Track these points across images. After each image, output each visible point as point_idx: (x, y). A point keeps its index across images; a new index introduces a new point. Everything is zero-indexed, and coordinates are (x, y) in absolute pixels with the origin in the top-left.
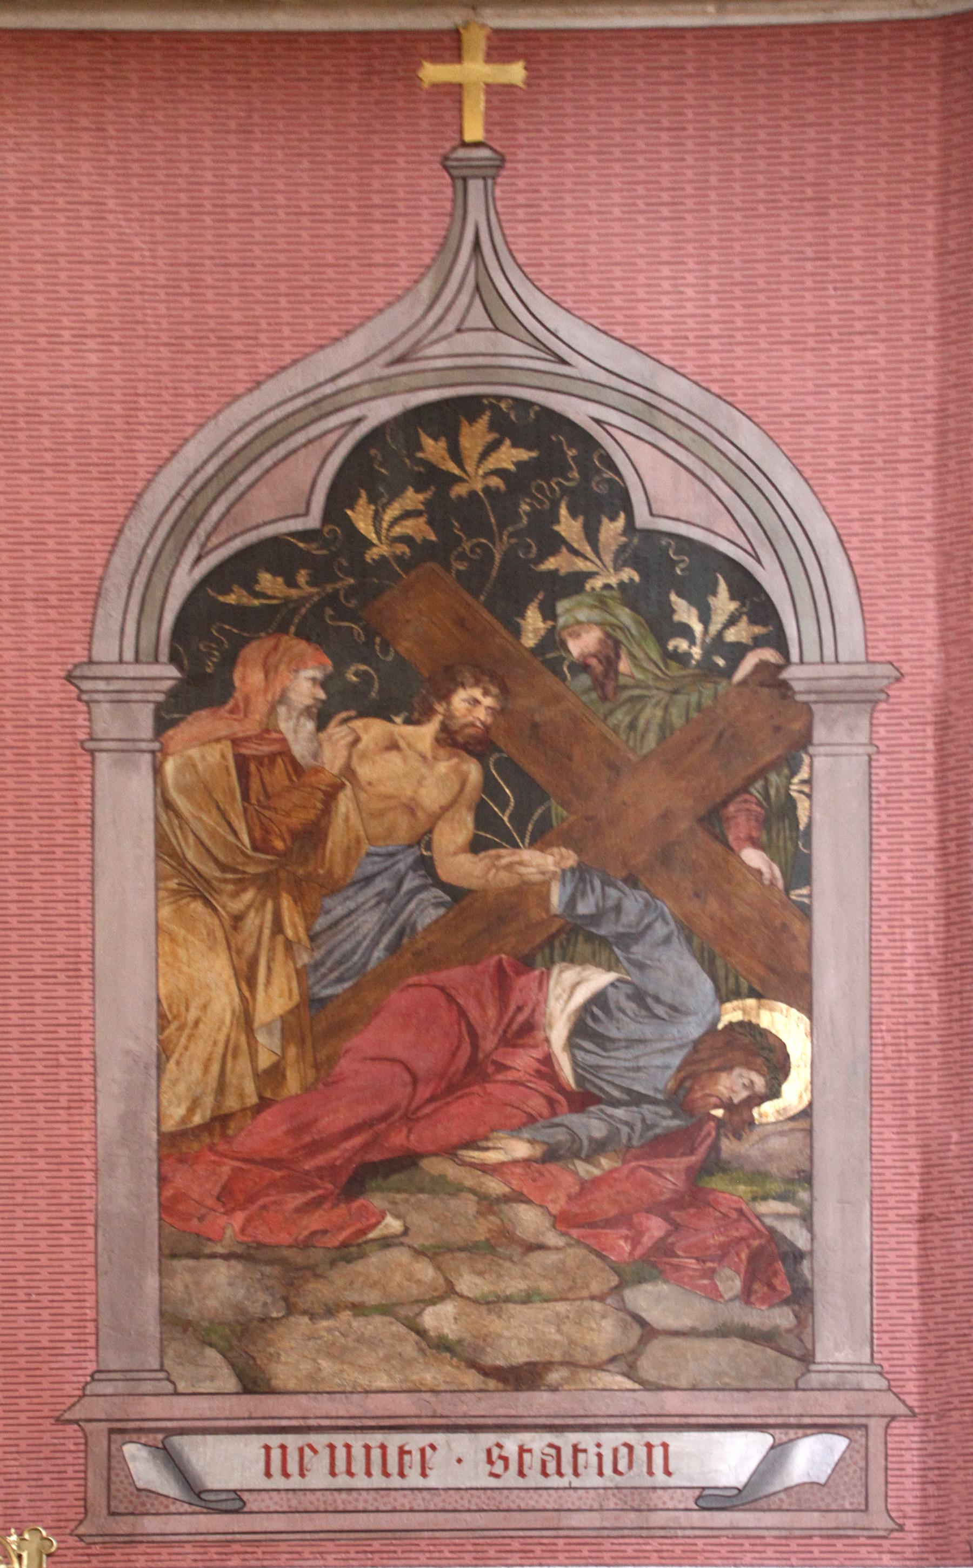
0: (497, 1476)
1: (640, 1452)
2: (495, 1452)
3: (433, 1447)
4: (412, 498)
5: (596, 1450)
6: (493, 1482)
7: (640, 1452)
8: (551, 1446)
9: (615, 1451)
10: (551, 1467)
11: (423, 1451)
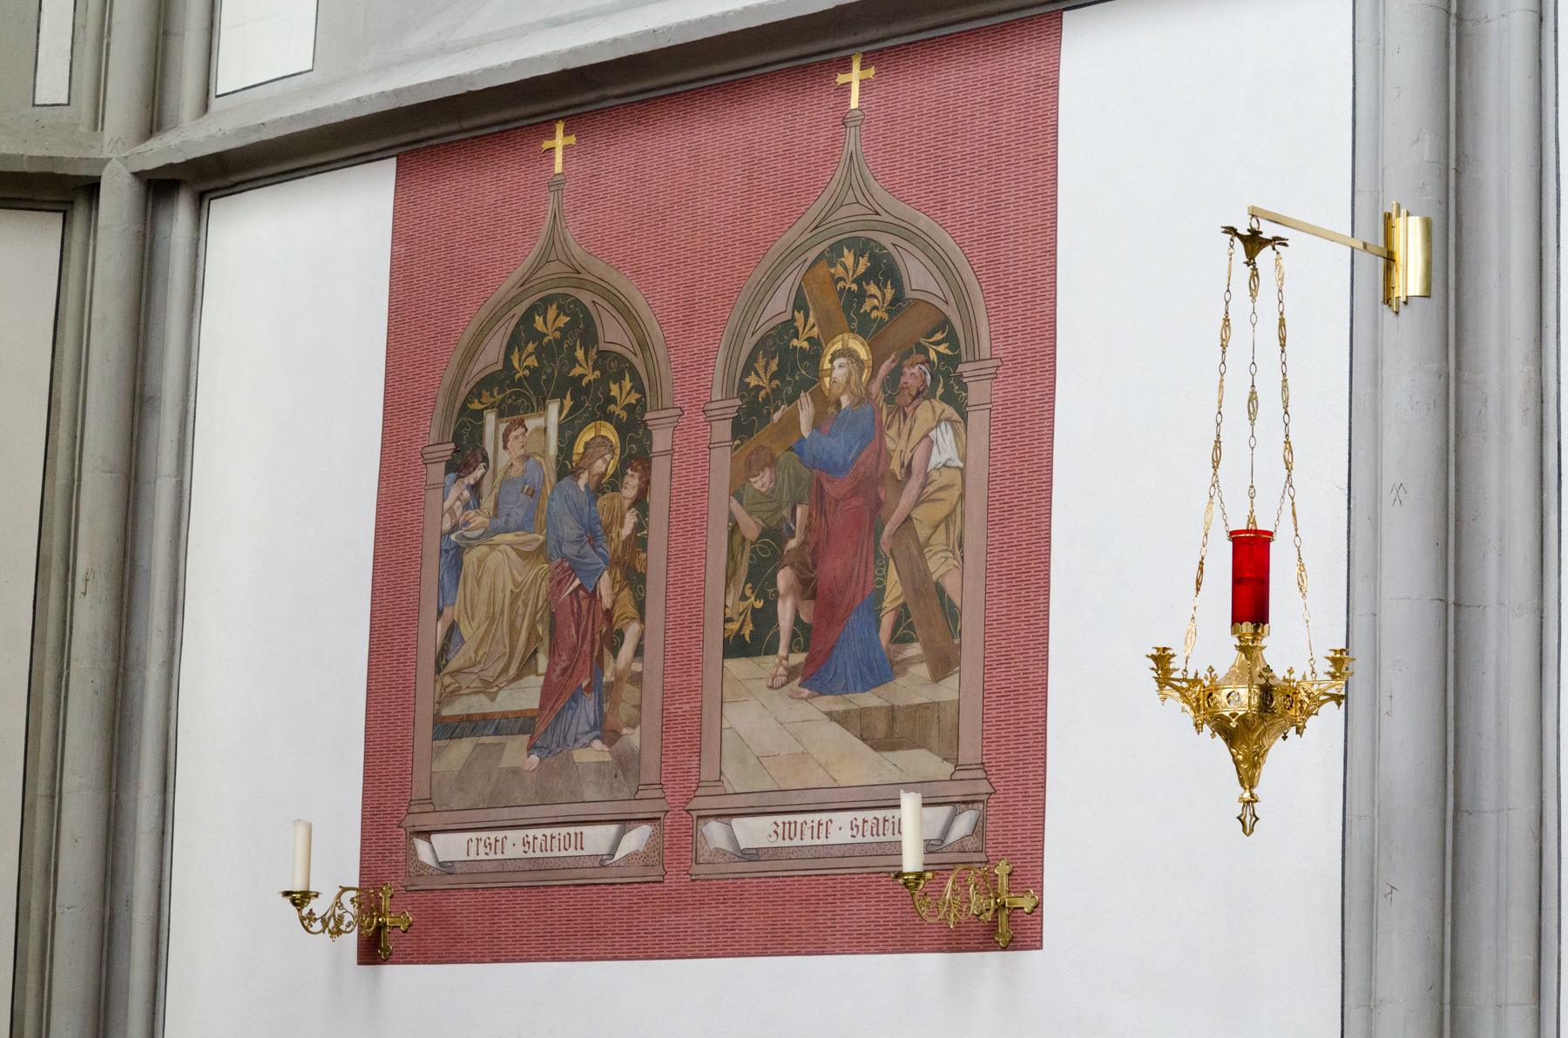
0: (526, 852)
6: (525, 856)
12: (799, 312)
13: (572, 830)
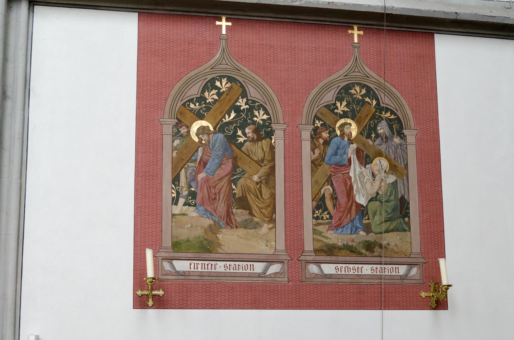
1: (249, 266)
2: (226, 265)
3: (217, 264)
4: (214, 92)
5: (242, 265)
7: (249, 266)
8: (235, 264)
9: (245, 266)
10: (235, 269)
11: (215, 265)
12: (338, 101)
13: (249, 263)
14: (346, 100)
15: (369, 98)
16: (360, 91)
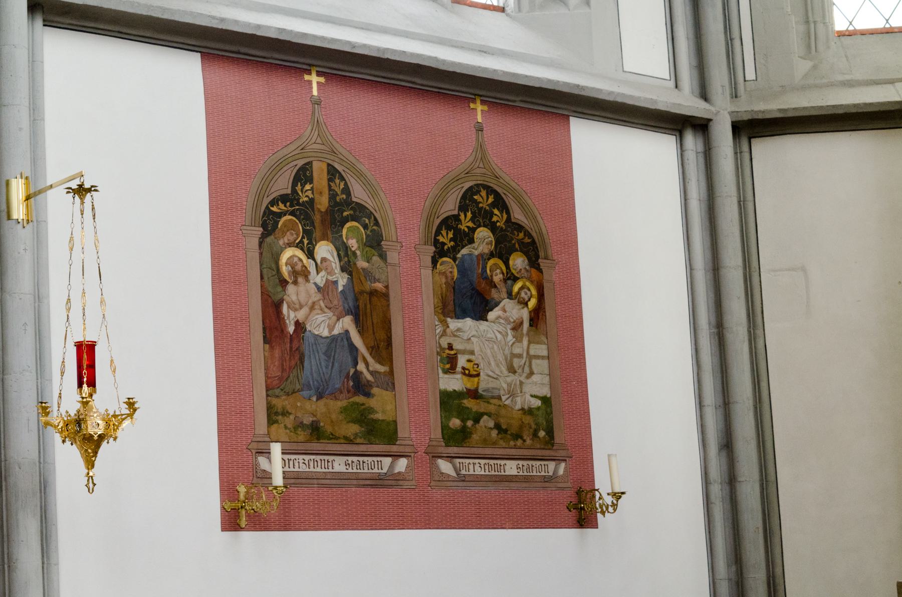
7: (376, 463)
8: (358, 461)
10: (358, 467)
11: (332, 461)
12: (462, 212)
13: (375, 459)
14: (471, 209)
15: (498, 210)
16: (488, 198)
